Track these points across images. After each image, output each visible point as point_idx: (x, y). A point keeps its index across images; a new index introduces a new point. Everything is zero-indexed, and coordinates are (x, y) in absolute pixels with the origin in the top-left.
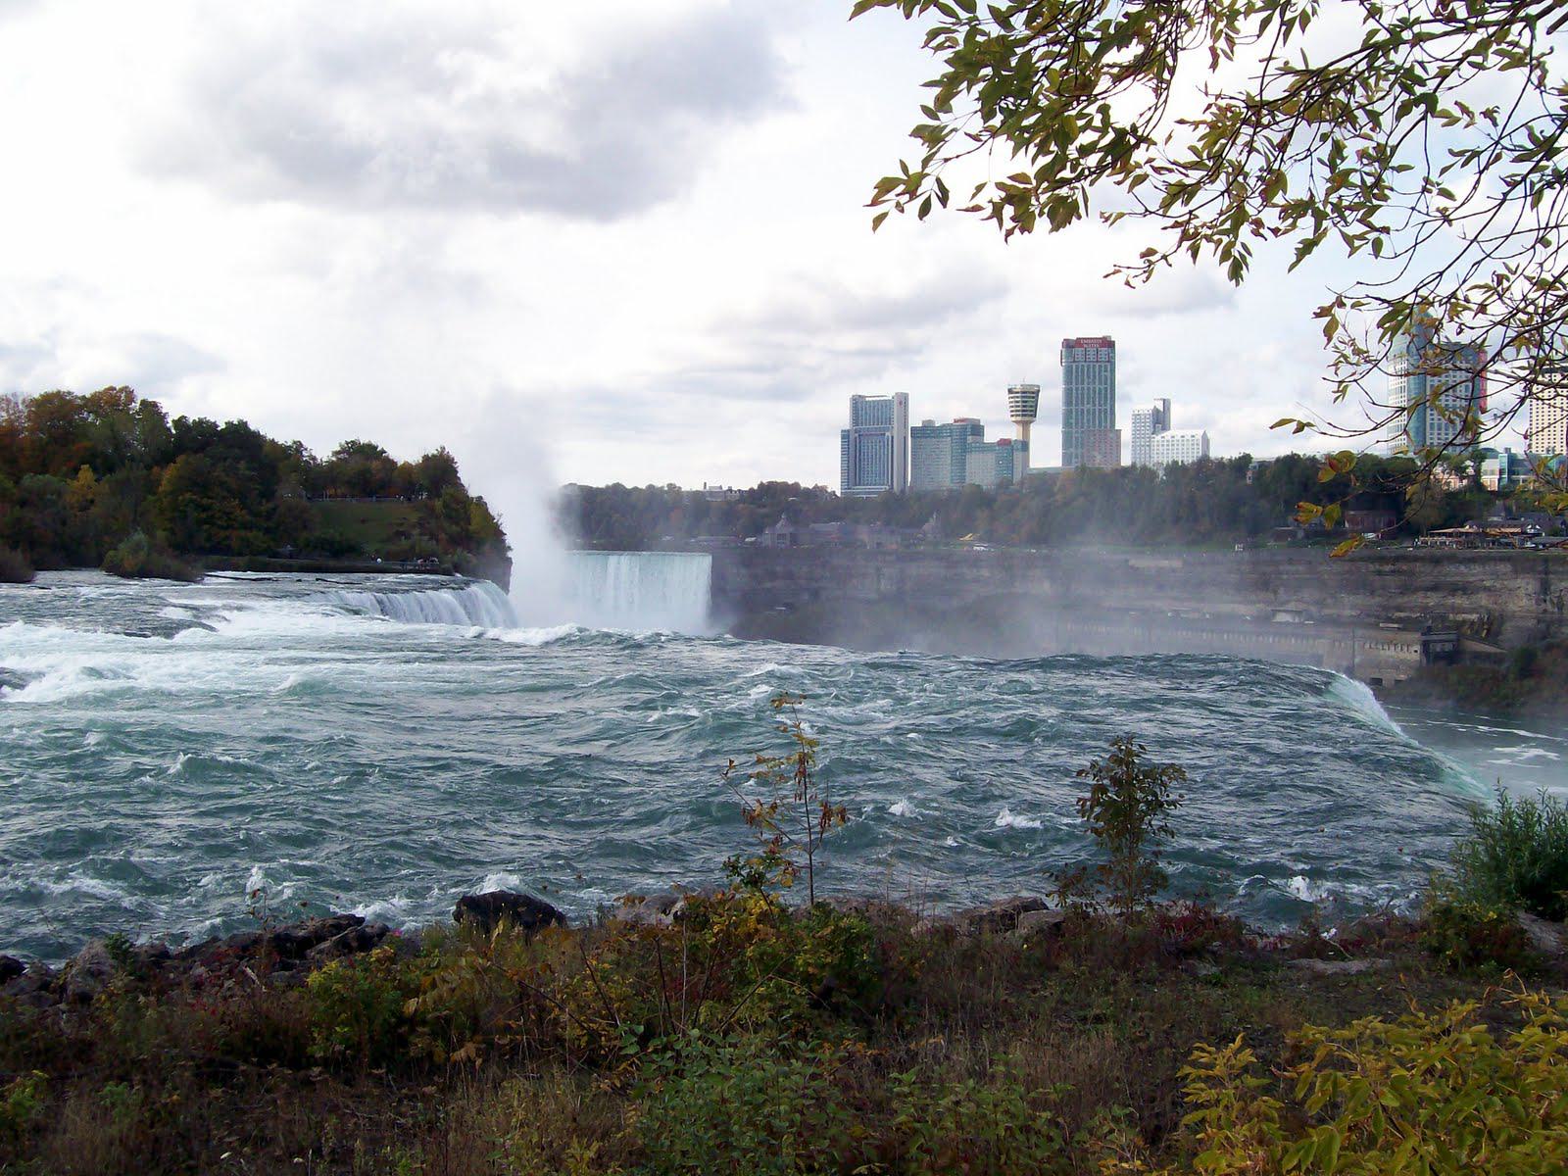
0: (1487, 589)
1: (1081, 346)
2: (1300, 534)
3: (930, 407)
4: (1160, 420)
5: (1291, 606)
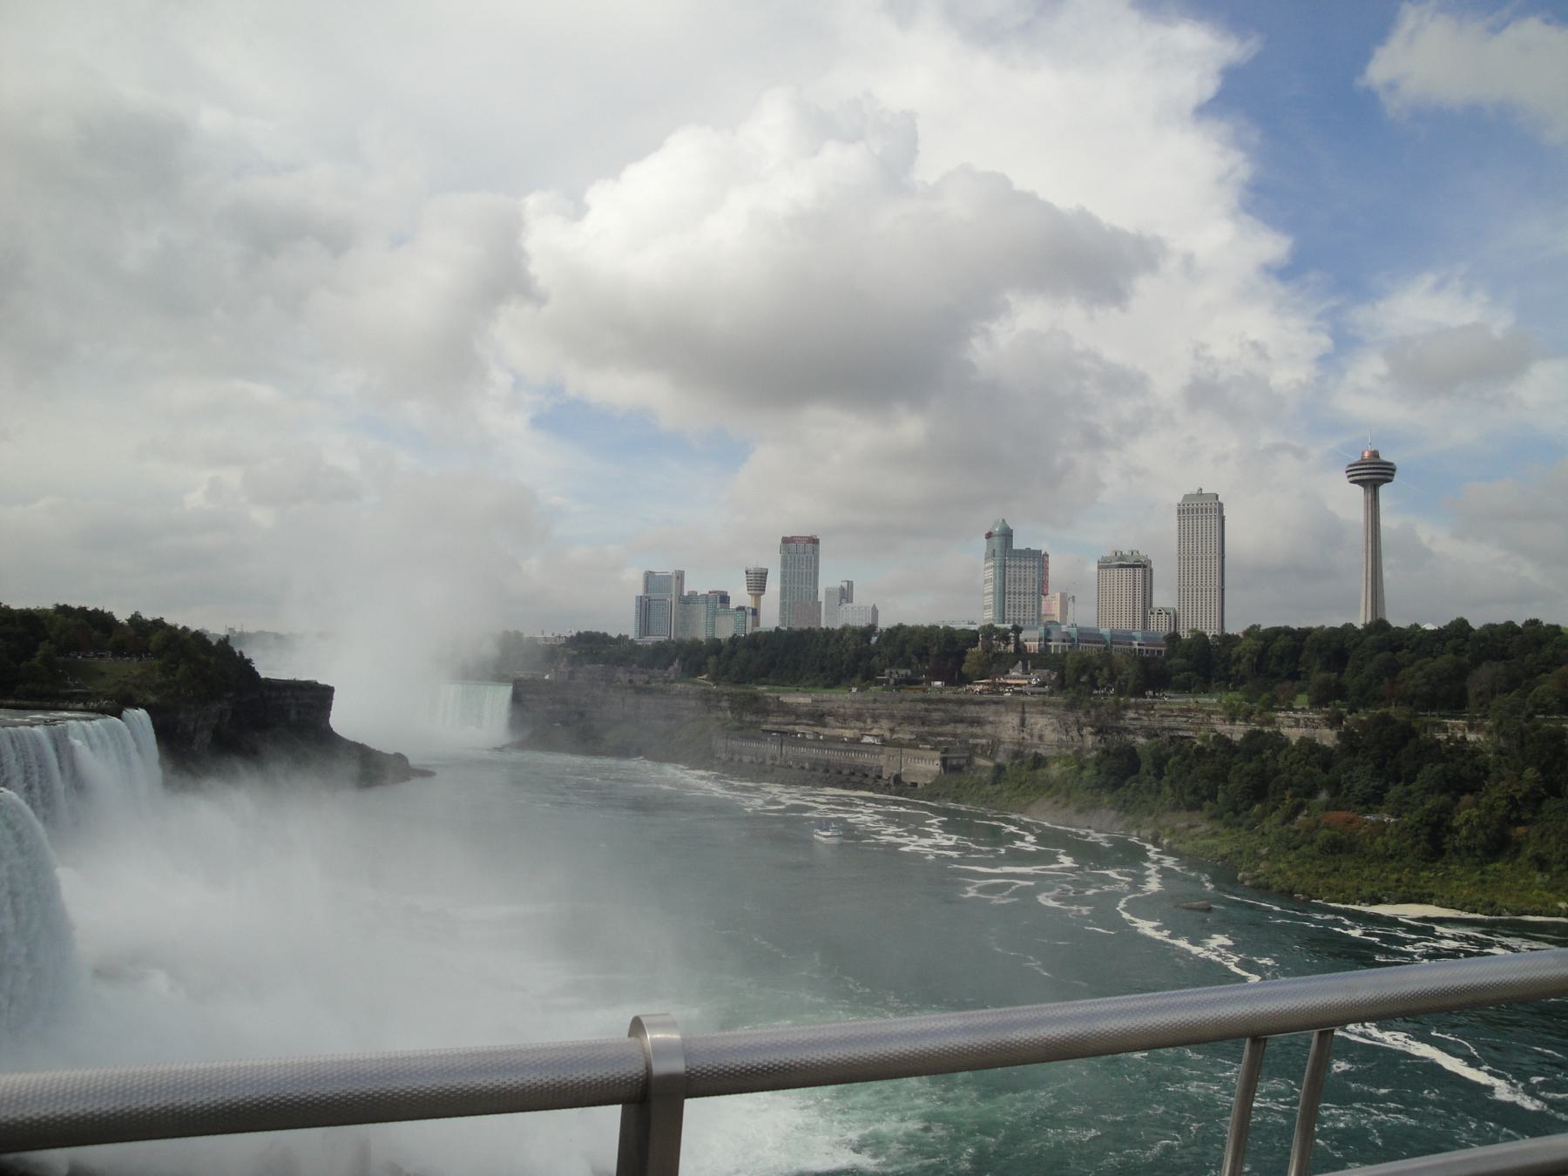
0: (991, 723)
1: (794, 542)
2: (892, 681)
3: (696, 584)
4: (845, 594)
5: (875, 732)
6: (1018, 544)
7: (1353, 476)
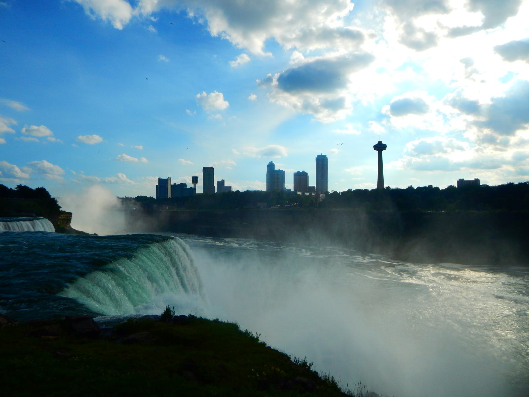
6: (276, 168)
7: (376, 148)
